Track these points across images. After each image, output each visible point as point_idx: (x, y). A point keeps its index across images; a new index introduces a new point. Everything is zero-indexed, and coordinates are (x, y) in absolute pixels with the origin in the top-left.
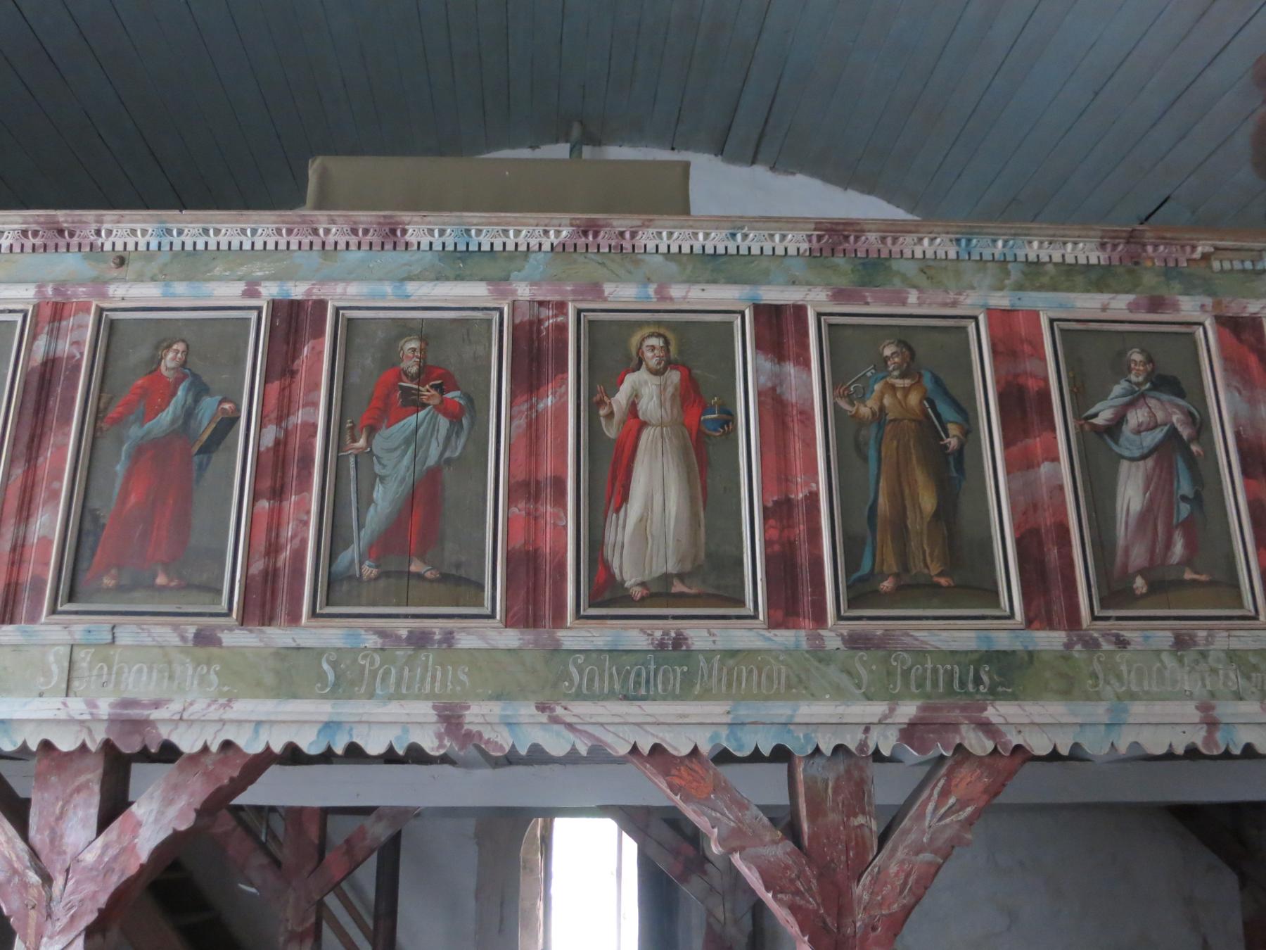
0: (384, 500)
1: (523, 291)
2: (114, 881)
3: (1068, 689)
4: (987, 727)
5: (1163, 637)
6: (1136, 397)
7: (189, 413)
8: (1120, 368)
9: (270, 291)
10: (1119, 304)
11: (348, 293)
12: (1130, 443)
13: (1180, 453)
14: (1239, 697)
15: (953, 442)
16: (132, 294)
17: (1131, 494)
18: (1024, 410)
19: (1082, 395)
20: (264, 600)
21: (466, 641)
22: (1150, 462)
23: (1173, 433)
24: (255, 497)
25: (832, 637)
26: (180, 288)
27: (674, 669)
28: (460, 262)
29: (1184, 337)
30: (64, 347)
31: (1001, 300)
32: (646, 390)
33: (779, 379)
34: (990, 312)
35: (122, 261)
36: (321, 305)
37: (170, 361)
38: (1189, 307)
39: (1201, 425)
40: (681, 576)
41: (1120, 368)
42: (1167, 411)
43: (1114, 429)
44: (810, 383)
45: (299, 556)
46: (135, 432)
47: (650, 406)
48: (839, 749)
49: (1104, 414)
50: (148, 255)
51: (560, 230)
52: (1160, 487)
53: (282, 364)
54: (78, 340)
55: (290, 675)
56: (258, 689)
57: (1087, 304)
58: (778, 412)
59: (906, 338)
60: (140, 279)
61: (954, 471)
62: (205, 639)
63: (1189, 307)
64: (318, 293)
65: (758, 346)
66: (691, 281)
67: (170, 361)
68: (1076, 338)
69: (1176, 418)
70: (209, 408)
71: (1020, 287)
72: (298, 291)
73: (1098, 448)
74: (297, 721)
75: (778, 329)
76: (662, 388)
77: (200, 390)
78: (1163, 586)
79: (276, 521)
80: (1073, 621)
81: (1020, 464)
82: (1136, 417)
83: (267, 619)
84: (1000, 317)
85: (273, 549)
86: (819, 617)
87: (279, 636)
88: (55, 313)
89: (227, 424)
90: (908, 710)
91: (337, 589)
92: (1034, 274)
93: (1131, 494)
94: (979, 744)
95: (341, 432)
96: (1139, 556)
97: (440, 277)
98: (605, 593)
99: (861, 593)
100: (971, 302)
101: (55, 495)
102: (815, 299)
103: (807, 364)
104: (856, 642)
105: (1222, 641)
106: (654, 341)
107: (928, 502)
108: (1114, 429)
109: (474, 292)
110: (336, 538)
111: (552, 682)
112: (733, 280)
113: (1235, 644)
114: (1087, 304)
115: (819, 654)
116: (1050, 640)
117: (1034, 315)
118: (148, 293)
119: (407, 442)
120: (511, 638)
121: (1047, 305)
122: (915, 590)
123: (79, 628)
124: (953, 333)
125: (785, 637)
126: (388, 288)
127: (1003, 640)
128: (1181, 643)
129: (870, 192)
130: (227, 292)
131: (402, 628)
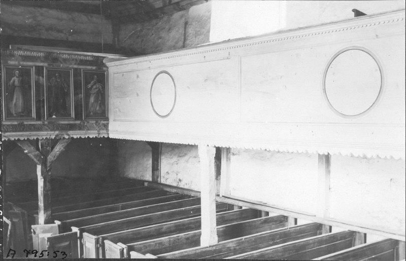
3: (80, 129)
4: (68, 135)
6: (95, 84)
8: (93, 79)
14: (103, 130)
15: (66, 91)
19: (87, 83)
22: (95, 95)
25: (46, 123)
31: (75, 66)
32: (16, 80)
33: (39, 79)
40: (22, 112)
44: (44, 80)
47: (17, 83)
58: (38, 85)
66: (24, 61)
75: (39, 70)
81: (76, 94)
84: (75, 70)
93: (92, 100)
94: (67, 137)
103: (43, 77)
105: (102, 122)
106: (17, 72)
113: (104, 122)
115: (44, 125)
125: (39, 122)
127: (72, 122)
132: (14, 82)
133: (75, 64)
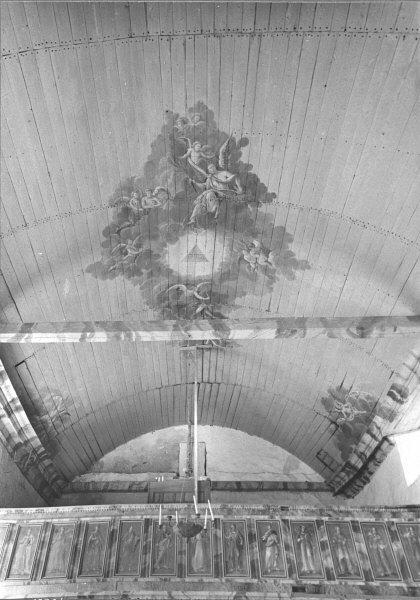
9: (145, 517)
10: (266, 517)
12: (269, 543)
20: (143, 575)
21: (172, 580)
25: (224, 580)
42: (273, 537)
44: (220, 533)
49: (264, 538)
53: (146, 531)
54: (117, 526)
57: (262, 517)
63: (277, 518)
68: (259, 523)
70: (136, 538)
72: (148, 517)
88: (113, 523)
90: (234, 593)
92: (254, 512)
93: (268, 553)
95: (154, 542)
104: (227, 580)
108: (265, 541)
110: (154, 562)
114: (262, 517)
116: (255, 581)
118: (127, 517)
120: (178, 580)
121: (255, 517)
125: (216, 579)
127: (248, 581)
128: (275, 582)
130: (139, 517)
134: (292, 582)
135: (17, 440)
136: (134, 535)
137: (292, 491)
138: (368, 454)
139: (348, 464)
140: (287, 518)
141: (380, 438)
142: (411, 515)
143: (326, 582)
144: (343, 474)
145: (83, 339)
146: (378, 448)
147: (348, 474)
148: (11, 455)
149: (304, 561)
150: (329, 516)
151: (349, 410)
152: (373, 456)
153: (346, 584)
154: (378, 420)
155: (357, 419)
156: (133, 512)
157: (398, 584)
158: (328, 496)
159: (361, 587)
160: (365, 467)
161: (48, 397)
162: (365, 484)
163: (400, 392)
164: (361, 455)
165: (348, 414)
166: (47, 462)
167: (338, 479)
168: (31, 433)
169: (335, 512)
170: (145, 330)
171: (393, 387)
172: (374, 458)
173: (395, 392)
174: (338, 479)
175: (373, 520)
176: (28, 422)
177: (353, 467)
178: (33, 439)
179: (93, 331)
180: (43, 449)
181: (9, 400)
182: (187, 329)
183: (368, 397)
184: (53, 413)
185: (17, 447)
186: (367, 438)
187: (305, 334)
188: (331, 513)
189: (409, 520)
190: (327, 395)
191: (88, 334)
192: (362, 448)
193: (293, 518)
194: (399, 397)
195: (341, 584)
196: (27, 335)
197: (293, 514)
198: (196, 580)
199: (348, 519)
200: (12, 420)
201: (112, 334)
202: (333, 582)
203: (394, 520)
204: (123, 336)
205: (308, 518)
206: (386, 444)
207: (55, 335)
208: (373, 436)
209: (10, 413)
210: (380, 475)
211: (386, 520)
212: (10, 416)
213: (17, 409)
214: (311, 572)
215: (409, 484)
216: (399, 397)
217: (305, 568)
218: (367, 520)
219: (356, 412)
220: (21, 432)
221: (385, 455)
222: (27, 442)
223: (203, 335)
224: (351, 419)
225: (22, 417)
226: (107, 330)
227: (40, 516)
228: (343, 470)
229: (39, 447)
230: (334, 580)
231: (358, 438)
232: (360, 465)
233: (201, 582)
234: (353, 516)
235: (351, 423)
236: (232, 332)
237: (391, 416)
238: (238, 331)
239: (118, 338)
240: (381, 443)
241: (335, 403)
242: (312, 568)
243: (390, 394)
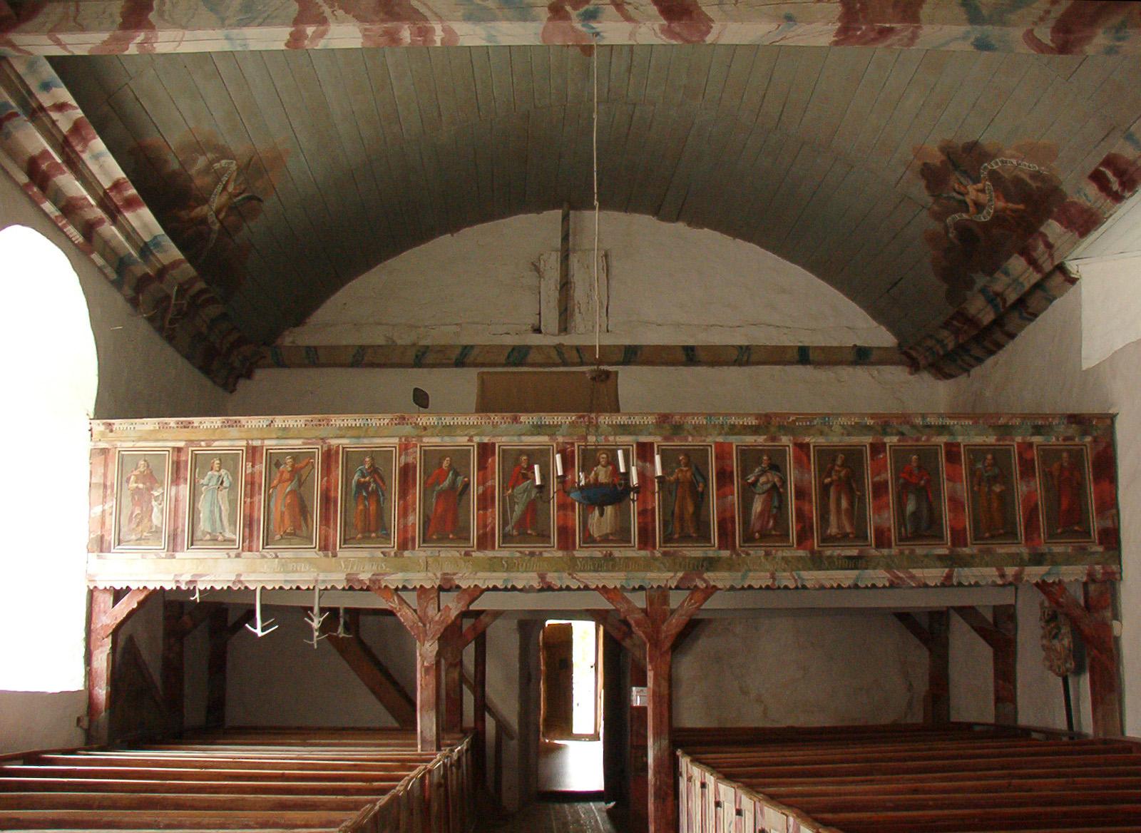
0: (518, 510)
1: (560, 439)
2: (444, 625)
4: (705, 581)
5: (763, 553)
6: (763, 472)
7: (454, 482)
8: (759, 462)
9: (477, 439)
10: (761, 439)
11: (502, 441)
12: (759, 489)
13: (776, 492)
14: (784, 570)
15: (700, 489)
16: (431, 441)
17: (757, 506)
18: (724, 477)
19: (745, 472)
20: (485, 541)
21: (546, 555)
22: (764, 496)
23: (774, 486)
24: (478, 510)
25: (658, 554)
26: (447, 439)
27: (608, 563)
28: (538, 429)
29: (782, 452)
30: (410, 460)
31: (720, 439)
34: (716, 443)
35: (425, 428)
36: (494, 444)
37: (445, 464)
38: (785, 440)
39: (784, 482)
40: (611, 534)
41: (759, 462)
42: (774, 477)
43: (754, 484)
45: (493, 529)
46: (438, 488)
48: (659, 587)
49: (751, 479)
50: (434, 427)
51: (572, 417)
52: (767, 504)
53: (482, 466)
54: (416, 457)
55: (493, 565)
56: (484, 570)
57: (750, 440)
59: (687, 453)
60: (432, 436)
61: (700, 499)
62: (467, 554)
63: (785, 440)
64: (493, 440)
65: (638, 458)
67: (445, 464)
68: (744, 452)
69: (776, 480)
71: (727, 434)
72: (486, 440)
73: (748, 492)
74: (497, 579)
76: (606, 472)
77: (456, 474)
78: (765, 536)
79: (485, 515)
80: (735, 546)
82: (763, 479)
83: (485, 548)
84: (719, 446)
85: (485, 526)
86: (654, 547)
87: (490, 554)
88: (405, 448)
89: (467, 485)
90: (680, 574)
91: (507, 538)
93: (757, 506)
94: (702, 585)
95: (504, 488)
96: (757, 527)
97: (532, 434)
98: (588, 539)
99: (667, 539)
100: (710, 440)
101: (415, 509)
102: (656, 440)
104: (665, 554)
105: (780, 554)
106: (604, 456)
107: (691, 509)
108: (754, 484)
109: (544, 439)
110: (505, 523)
111: (573, 566)
112: (630, 434)
113: (784, 554)
114: (750, 440)
115: (654, 558)
116: (726, 553)
117: (731, 444)
118: (437, 440)
119: (524, 492)
120: (560, 554)
121: (735, 440)
122: (685, 538)
123: (429, 552)
124: (704, 451)
125: (643, 553)
126: (515, 438)
127: (711, 554)
128: (767, 554)
129: (750, 240)
131: (527, 551)
132: (597, 475)
133: (720, 434)
134: (801, 553)
135: (142, 269)
136: (456, 474)
137: (818, 364)
138: (1012, 297)
139: (962, 316)
140: (807, 440)
141: (1048, 267)
142: (1073, 430)
143: (873, 552)
144: (945, 333)
145: (296, 40)
146: (1038, 286)
147: (957, 333)
148: (134, 302)
149: (833, 519)
150: (902, 434)
151: (983, 198)
152: (1021, 302)
153: (912, 552)
154: (1053, 229)
155: (999, 219)
156: (449, 430)
157: (1014, 549)
158: (897, 374)
159: (940, 558)
160: (998, 322)
161: (202, 162)
162: (991, 353)
163: (1120, 173)
164: (993, 299)
165: (979, 207)
166: (213, 311)
167: (930, 343)
168: (172, 252)
169: (914, 426)
170: (468, 18)
171: (1109, 162)
172: (1027, 306)
173: (1109, 174)
174: (930, 343)
175: (992, 439)
176: (158, 230)
177: (971, 321)
178: (175, 264)
179: (322, 21)
180: (201, 285)
181: (107, 184)
182: (591, 16)
183: (1035, 176)
184: (217, 200)
185: (144, 281)
186: (1017, 264)
187: (913, 38)
188: (905, 429)
189: (1066, 439)
190: (936, 158)
191: (310, 30)
192: (1000, 283)
193: (821, 440)
194: (1116, 186)
195: (901, 553)
196: (141, 36)
197: (822, 433)
198: (597, 554)
199: (942, 440)
200: (122, 229)
201: (378, 28)
202: (885, 551)
203: (1037, 439)
204: (406, 34)
205: (854, 440)
206: (1058, 278)
207: (219, 33)
208: (1033, 262)
209: (113, 213)
210: (1033, 338)
211: (1019, 439)
212: (114, 221)
213: (130, 204)
214: (845, 536)
215: (1084, 369)
216: (1116, 186)
217: (833, 530)
218: (979, 440)
219: (1001, 204)
220: (145, 250)
221: (1051, 300)
222: (162, 272)
223: (632, 35)
224: (984, 217)
225: (144, 219)
226: (360, 18)
227: (234, 432)
228: (946, 325)
229: (192, 281)
230: (890, 546)
231: (993, 266)
232: (988, 317)
233: (609, 557)
234: (951, 434)
235: (984, 226)
236: (716, 27)
237: (1085, 223)
238: (733, 26)
239: (393, 38)
240: (1047, 276)
241: (955, 180)
242: (848, 530)
243: (1097, 177)
